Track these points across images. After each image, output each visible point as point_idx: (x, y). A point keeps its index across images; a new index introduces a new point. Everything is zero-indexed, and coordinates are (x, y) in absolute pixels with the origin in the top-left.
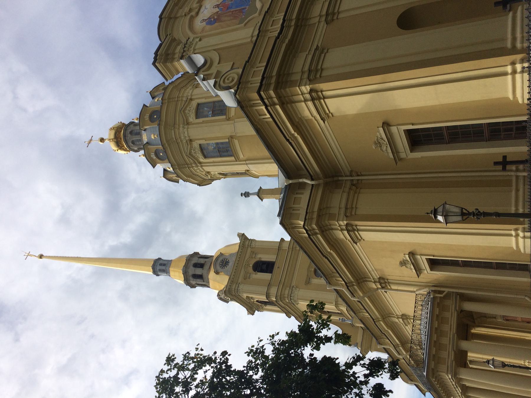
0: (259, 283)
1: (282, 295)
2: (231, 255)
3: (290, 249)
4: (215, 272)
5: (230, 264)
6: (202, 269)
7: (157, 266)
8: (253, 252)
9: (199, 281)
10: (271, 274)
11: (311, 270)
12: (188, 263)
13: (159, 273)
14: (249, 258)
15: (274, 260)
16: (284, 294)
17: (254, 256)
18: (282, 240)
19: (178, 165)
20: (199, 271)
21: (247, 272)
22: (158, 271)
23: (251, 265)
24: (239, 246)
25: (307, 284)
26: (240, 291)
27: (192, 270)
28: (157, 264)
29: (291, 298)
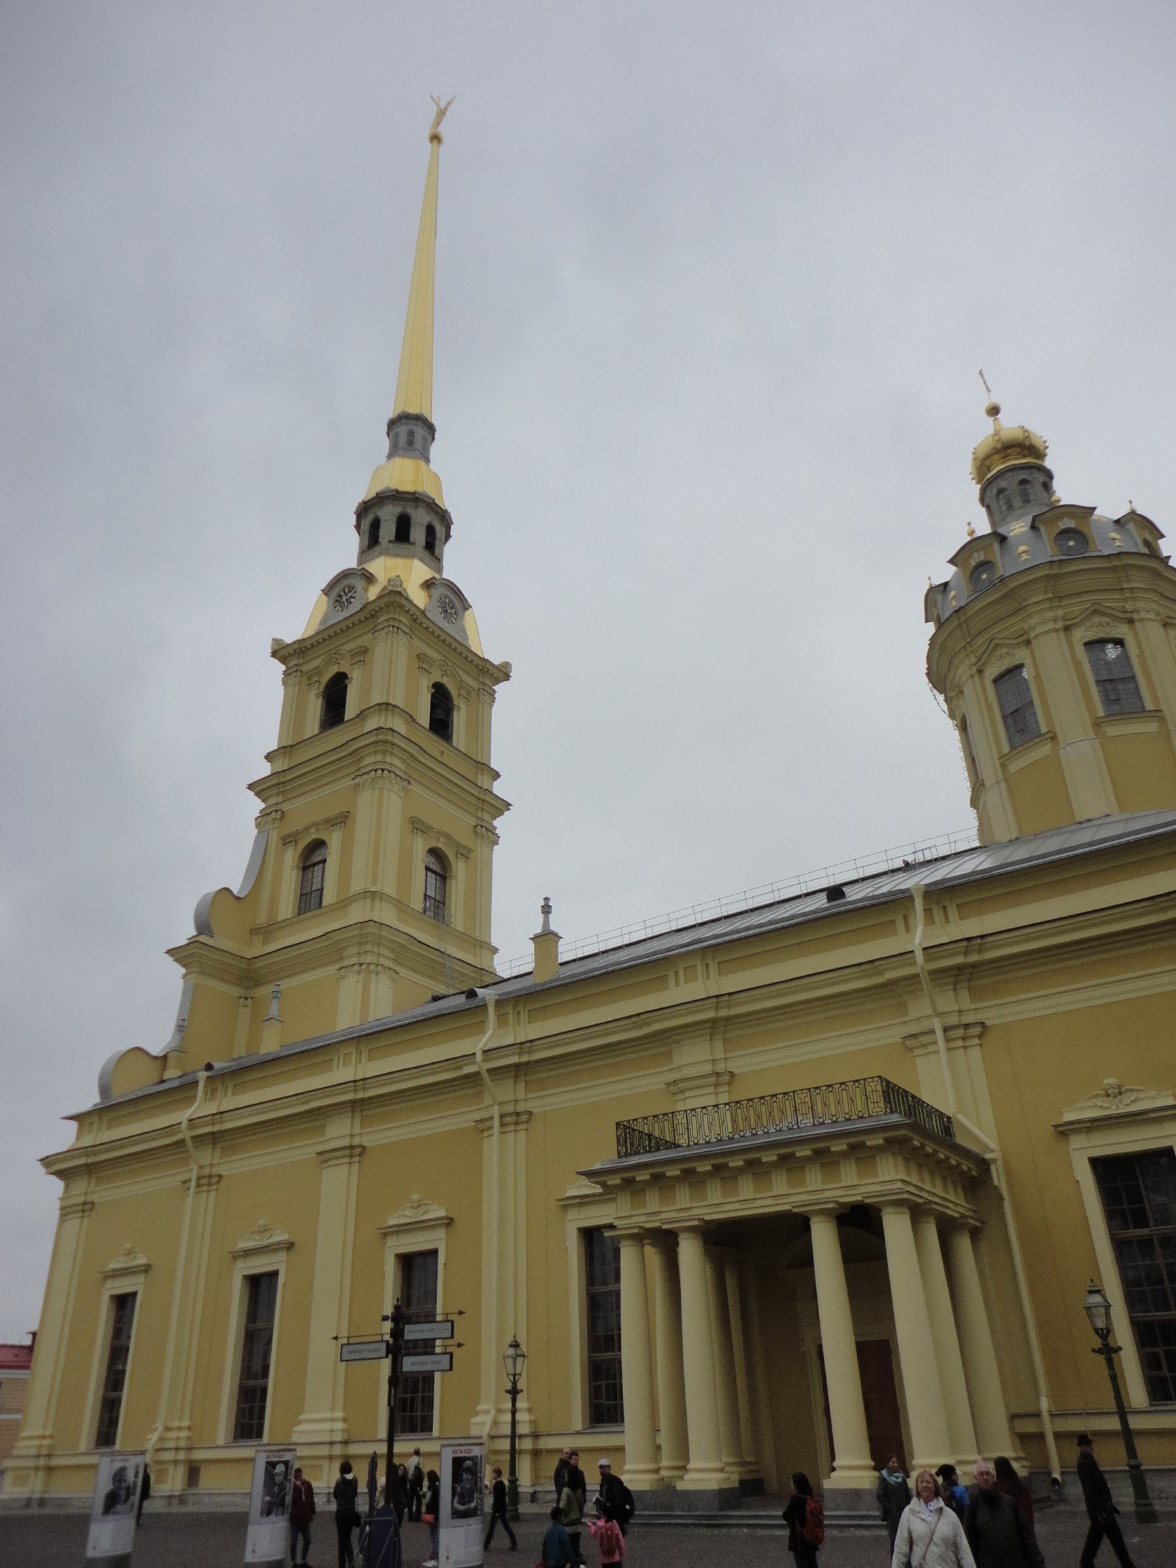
1: (392, 749)
3: (484, 795)
4: (434, 581)
6: (424, 544)
9: (388, 531)
11: (441, 839)
12: (436, 512)
13: (403, 430)
14: (462, 681)
15: (454, 745)
16: (392, 754)
18: (496, 775)
21: (432, 665)
23: (446, 681)
24: (487, 660)
25: (412, 823)
26: (395, 635)
29: (386, 772)
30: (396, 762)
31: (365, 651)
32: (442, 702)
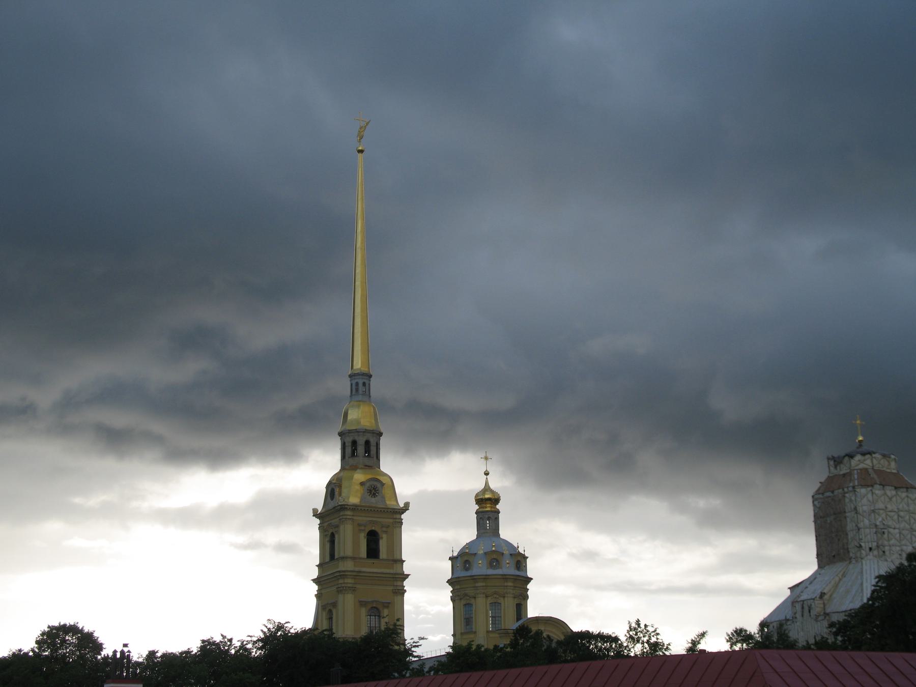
0: (356, 544)
2: (383, 497)
5: (373, 500)
7: (362, 378)
8: (388, 527)
9: (349, 450)
10: (366, 557)
12: (369, 432)
15: (381, 558)
17: (384, 529)
19: (459, 581)
20: (361, 449)
22: (356, 381)
23: (373, 528)
27: (361, 441)
28: (364, 379)
30: (350, 581)
31: (337, 526)
32: (373, 538)
